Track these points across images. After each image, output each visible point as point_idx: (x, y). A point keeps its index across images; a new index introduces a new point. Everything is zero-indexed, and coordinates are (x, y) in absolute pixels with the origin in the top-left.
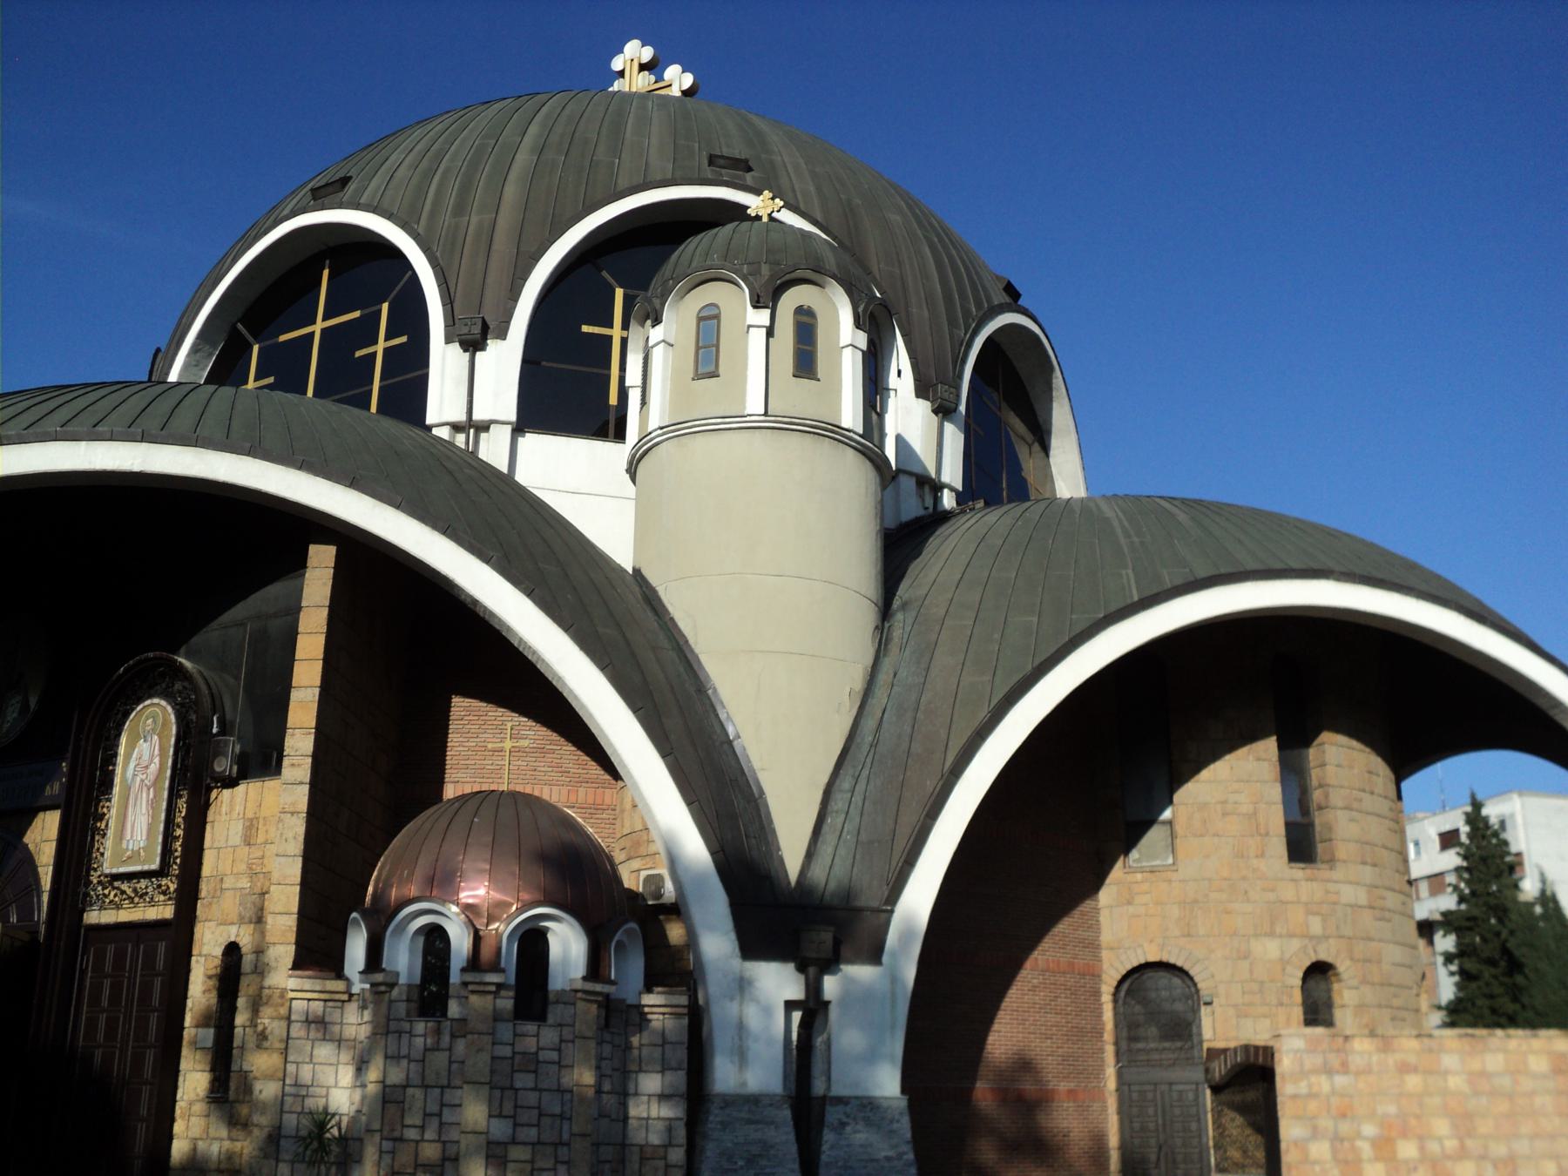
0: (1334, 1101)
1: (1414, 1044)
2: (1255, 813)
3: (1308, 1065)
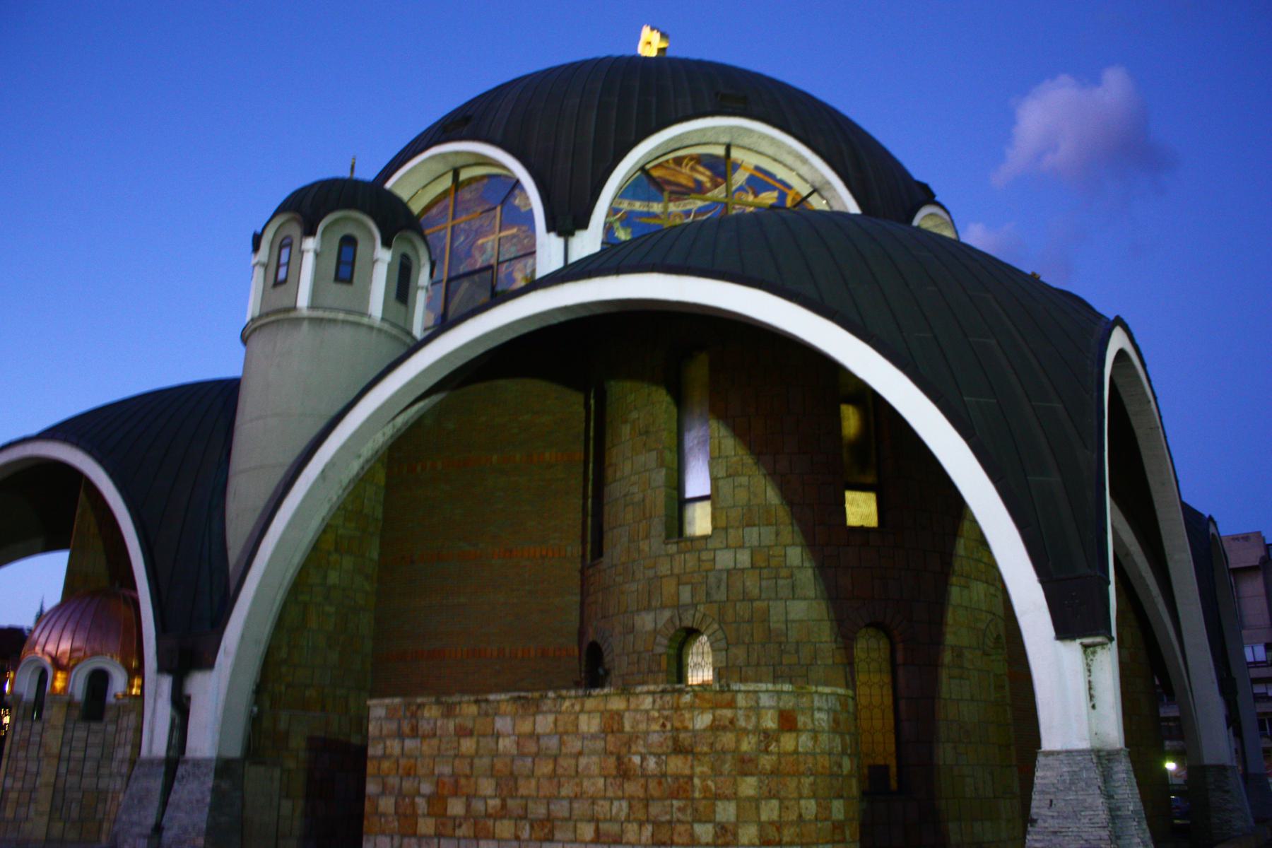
0: (403, 762)
1: (473, 709)
2: (644, 500)
3: (385, 732)
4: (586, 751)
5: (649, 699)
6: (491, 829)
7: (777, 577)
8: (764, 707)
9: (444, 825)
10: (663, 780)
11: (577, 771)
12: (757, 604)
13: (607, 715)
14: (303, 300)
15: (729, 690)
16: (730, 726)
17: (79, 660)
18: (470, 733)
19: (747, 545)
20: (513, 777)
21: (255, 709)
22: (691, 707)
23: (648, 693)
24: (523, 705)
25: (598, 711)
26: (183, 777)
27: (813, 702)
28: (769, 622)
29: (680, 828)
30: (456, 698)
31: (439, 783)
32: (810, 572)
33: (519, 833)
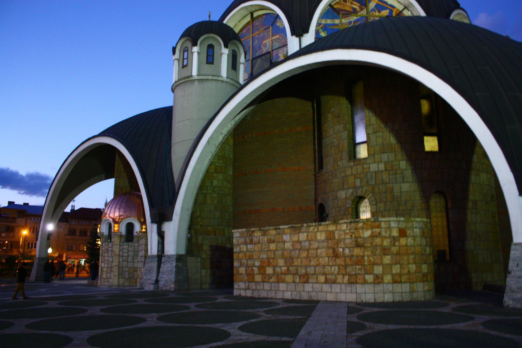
0: (247, 253)
1: (274, 232)
2: (339, 144)
3: (240, 242)
4: (320, 247)
5: (345, 226)
6: (284, 279)
7: (396, 174)
8: (393, 227)
9: (265, 277)
10: (352, 258)
11: (317, 255)
12: (388, 185)
13: (328, 232)
14: (195, 72)
15: (378, 221)
16: (379, 235)
17: (122, 219)
18: (273, 242)
19: (383, 161)
20: (292, 258)
21: (189, 235)
22: (362, 228)
23: (345, 223)
24: (294, 230)
25: (324, 231)
26: (164, 262)
27: (413, 225)
28: (393, 192)
29: (360, 277)
30: (267, 228)
31: (262, 262)
32: (410, 171)
33: (295, 280)
